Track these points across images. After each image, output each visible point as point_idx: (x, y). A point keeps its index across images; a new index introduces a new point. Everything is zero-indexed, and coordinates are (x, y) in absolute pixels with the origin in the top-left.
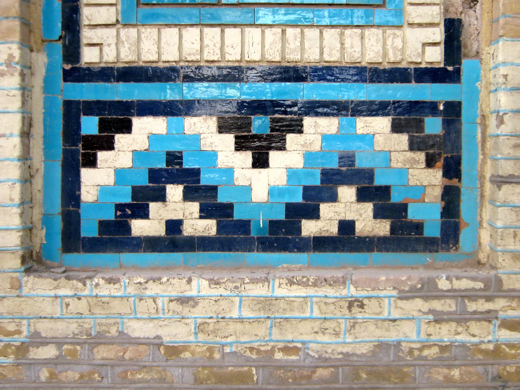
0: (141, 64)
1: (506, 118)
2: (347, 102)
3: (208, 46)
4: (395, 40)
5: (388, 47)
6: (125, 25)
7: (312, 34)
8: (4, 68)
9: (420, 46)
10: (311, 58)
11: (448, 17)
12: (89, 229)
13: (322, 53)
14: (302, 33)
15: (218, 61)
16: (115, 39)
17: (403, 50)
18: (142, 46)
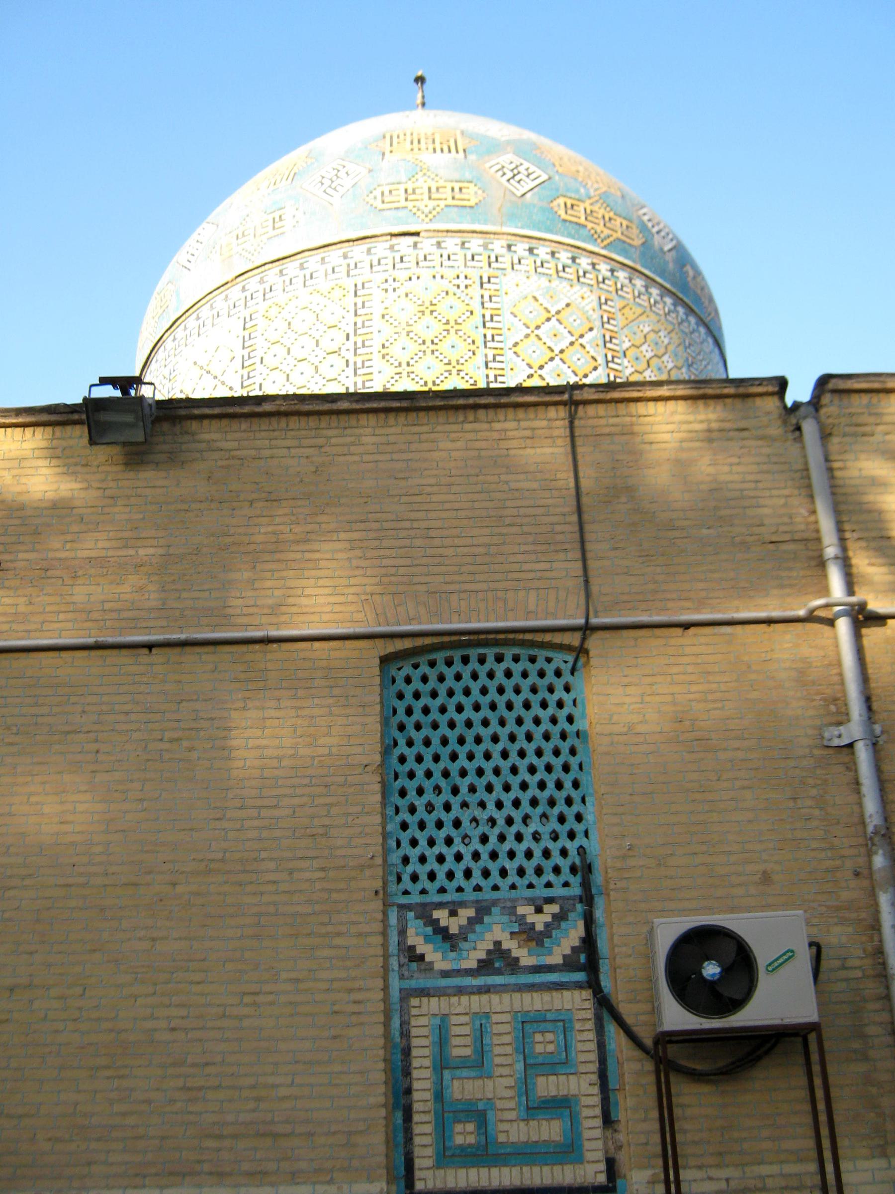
13: (542, 1179)
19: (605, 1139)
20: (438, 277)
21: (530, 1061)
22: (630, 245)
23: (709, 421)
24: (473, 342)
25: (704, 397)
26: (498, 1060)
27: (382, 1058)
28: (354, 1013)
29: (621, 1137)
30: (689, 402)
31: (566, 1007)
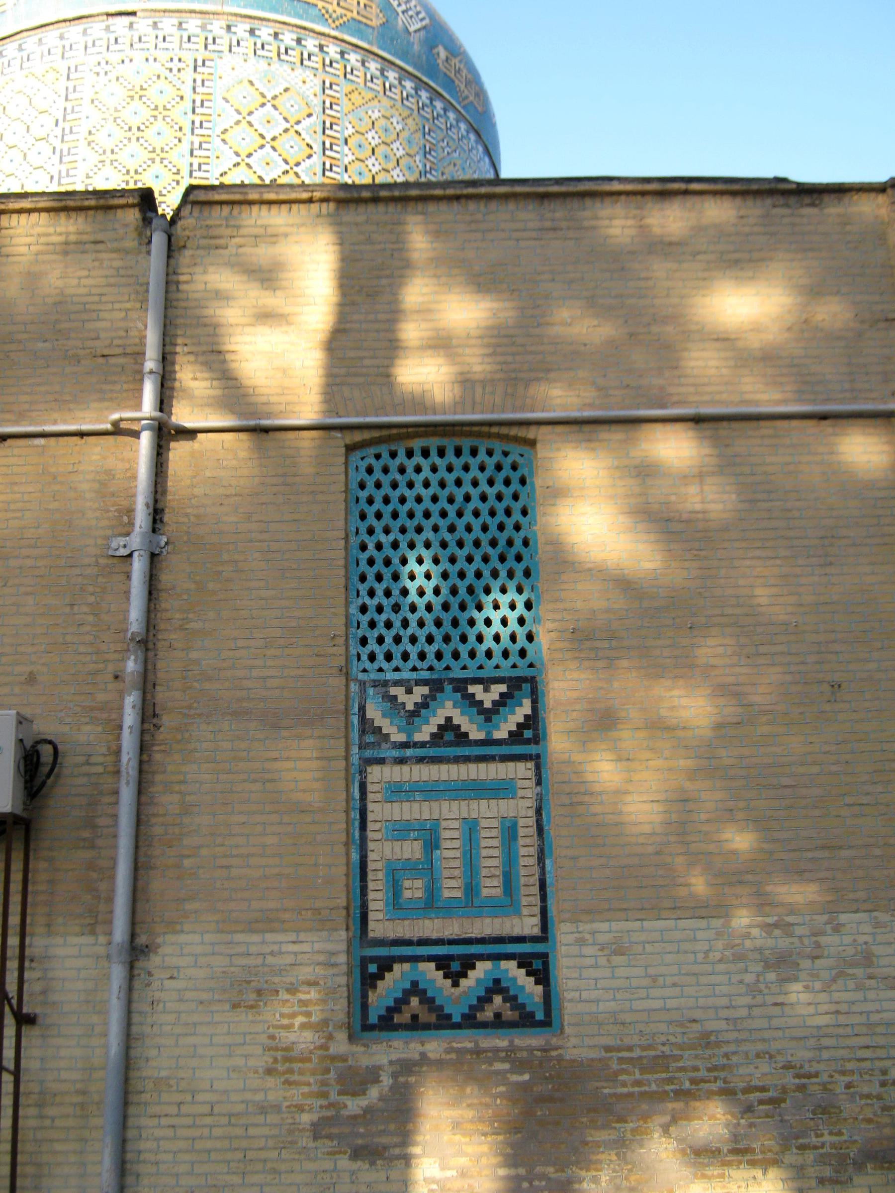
12: (373, 1019)
20: (151, 59)
22: (366, 24)
23: (68, 234)
24: (181, 129)
25: (66, 209)
30: (52, 214)
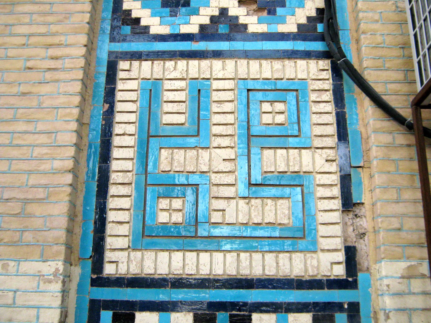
0: (143, 276)
1: (391, 315)
2: (281, 303)
3: (188, 264)
4: (312, 261)
5: (308, 265)
6: (133, 249)
7: (257, 257)
8: (51, 277)
9: (329, 264)
10: (257, 273)
11: (347, 245)
13: (264, 270)
14: (251, 256)
15: (195, 275)
16: (127, 258)
17: (318, 268)
18: (144, 263)
19: (345, 224)
21: (254, 131)
26: (216, 130)
27: (76, 117)
28: (49, 69)
29: (365, 223)
31: (299, 77)
